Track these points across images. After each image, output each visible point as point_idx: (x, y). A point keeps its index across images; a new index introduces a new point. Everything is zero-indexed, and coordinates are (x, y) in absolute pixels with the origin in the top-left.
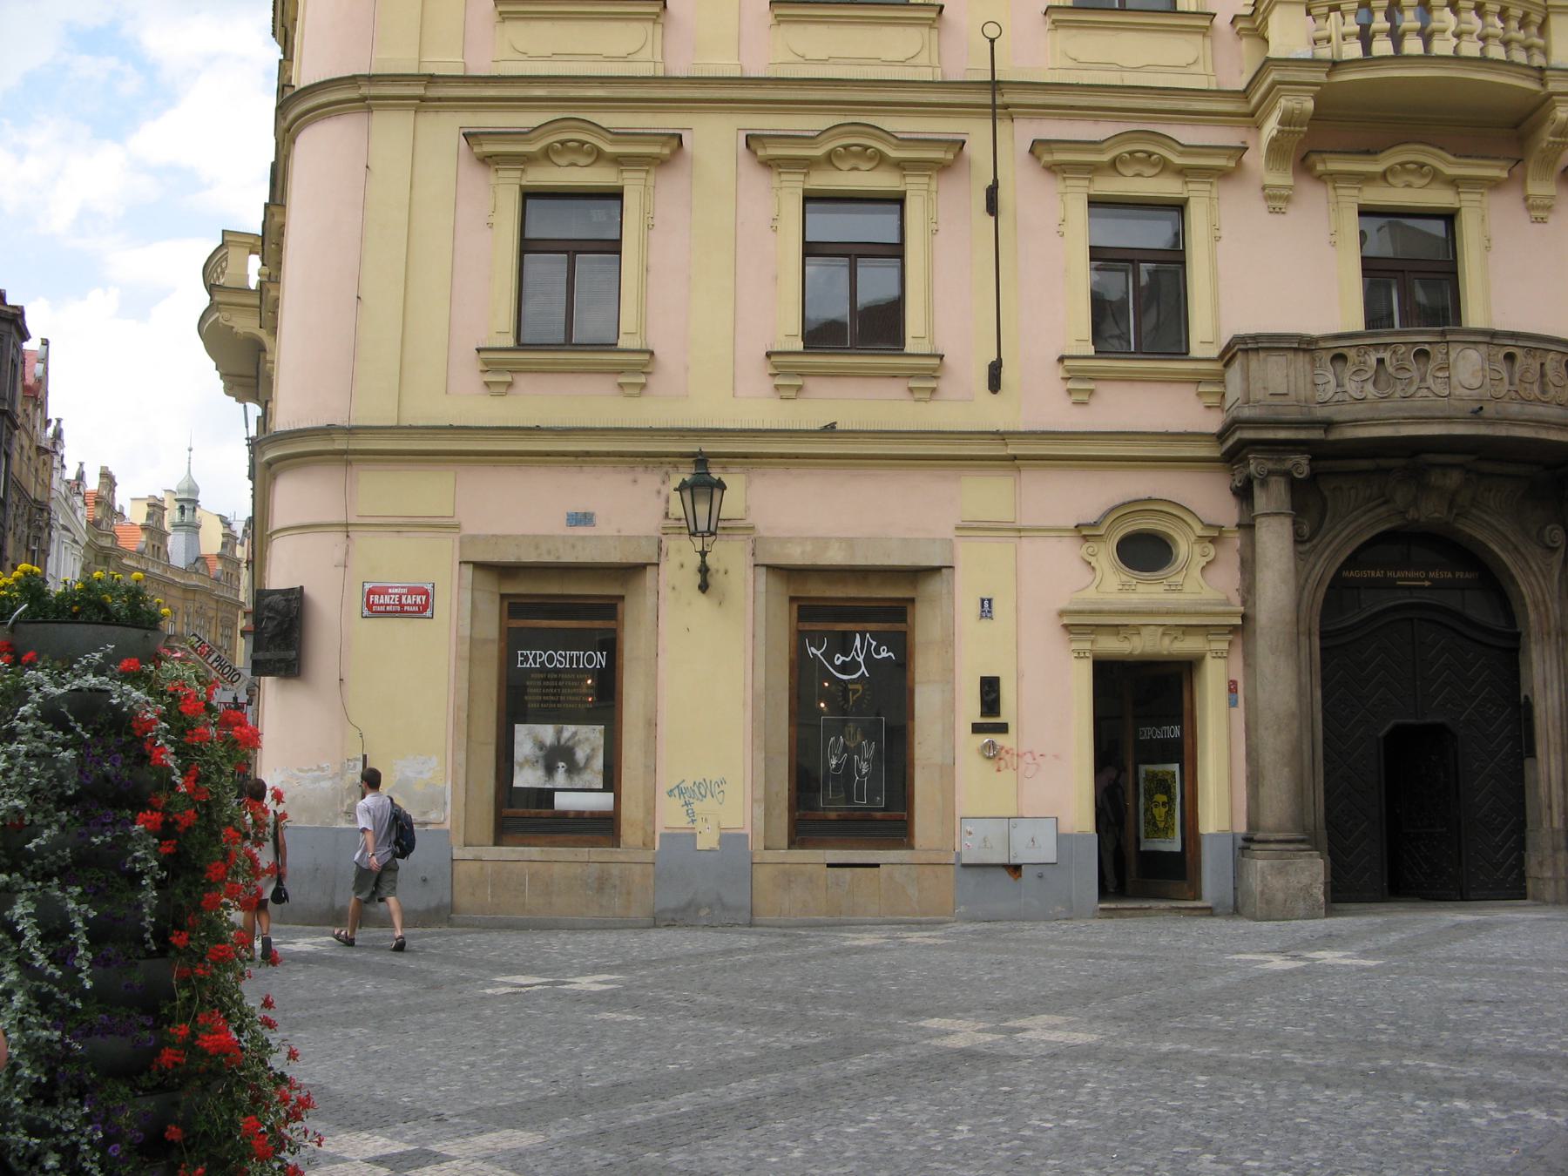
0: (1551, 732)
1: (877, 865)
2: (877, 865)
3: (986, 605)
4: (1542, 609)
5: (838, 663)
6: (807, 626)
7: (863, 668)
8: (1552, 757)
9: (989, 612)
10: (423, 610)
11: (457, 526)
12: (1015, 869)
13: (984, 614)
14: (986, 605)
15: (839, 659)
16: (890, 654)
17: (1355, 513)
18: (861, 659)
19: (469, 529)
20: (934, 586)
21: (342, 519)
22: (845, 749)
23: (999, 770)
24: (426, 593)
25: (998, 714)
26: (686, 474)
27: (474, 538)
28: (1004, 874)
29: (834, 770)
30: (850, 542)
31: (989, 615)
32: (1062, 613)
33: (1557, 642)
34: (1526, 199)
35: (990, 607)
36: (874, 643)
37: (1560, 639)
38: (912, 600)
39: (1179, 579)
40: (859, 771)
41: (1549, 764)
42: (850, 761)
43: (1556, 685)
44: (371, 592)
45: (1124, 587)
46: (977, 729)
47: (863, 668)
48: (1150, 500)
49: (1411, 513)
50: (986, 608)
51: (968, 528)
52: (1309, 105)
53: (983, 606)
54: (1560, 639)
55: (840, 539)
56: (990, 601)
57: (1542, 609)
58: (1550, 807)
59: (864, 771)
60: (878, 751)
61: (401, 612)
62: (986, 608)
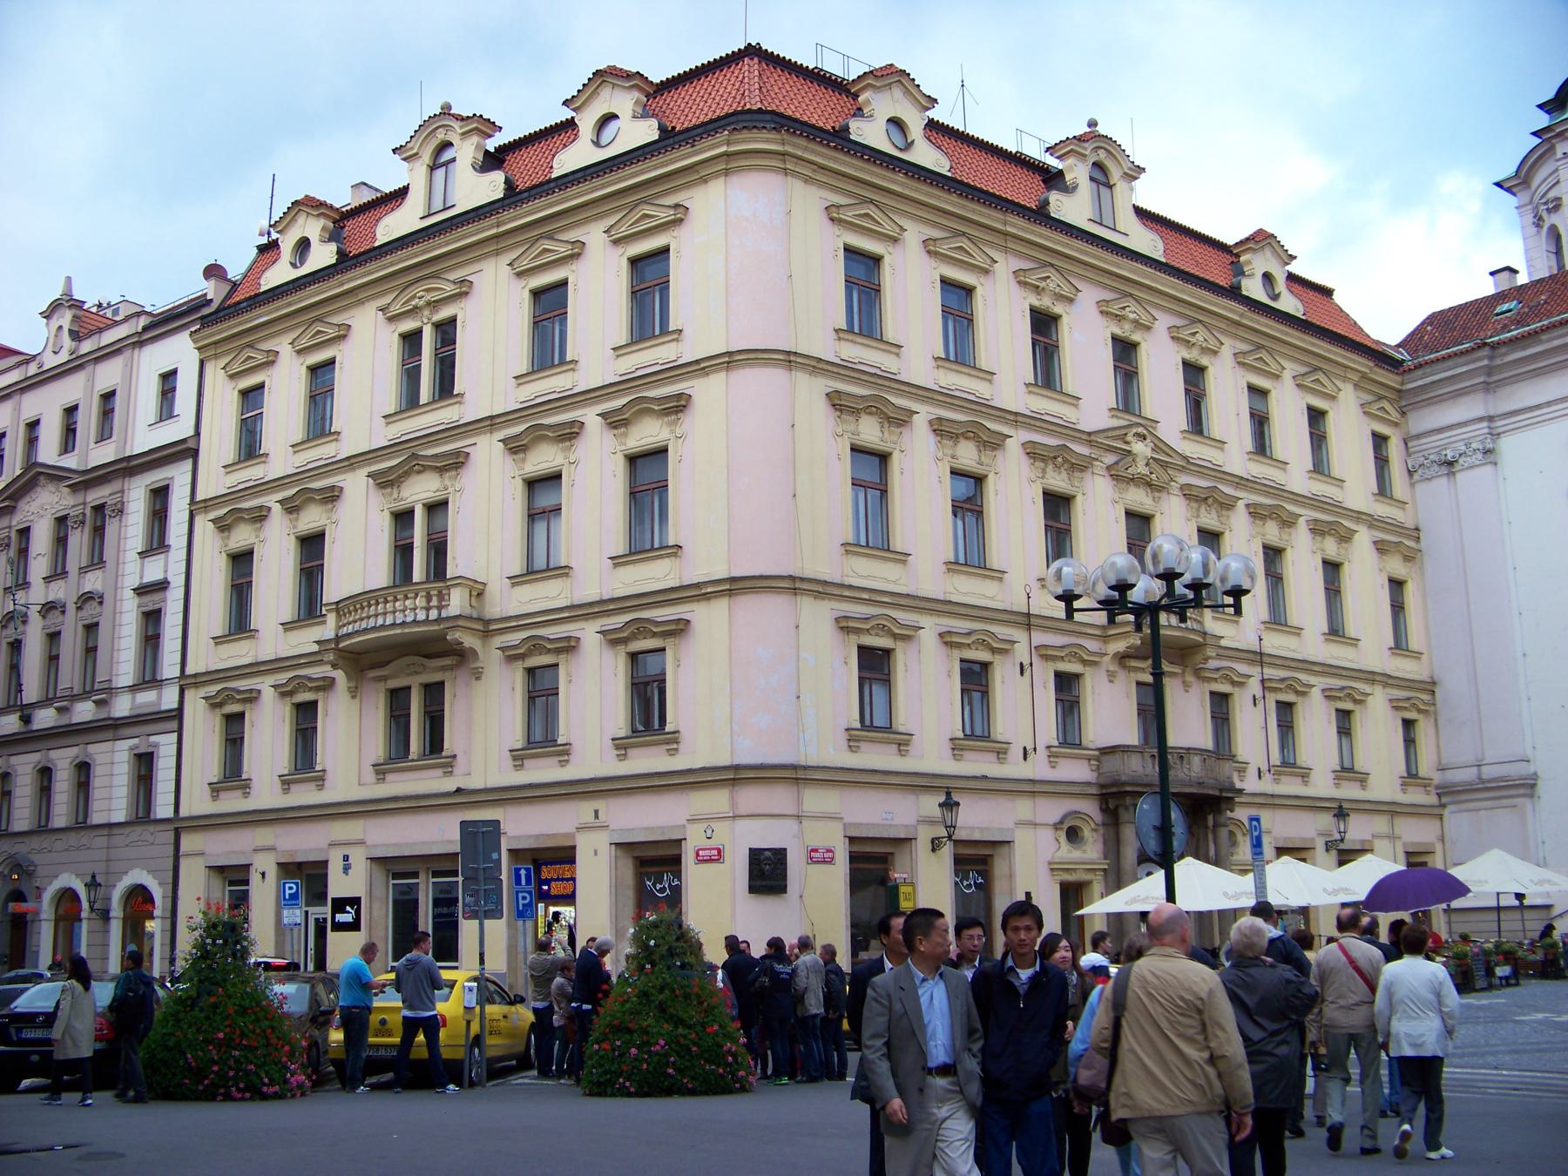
10: (831, 861)
11: (842, 818)
15: (965, 883)
19: (847, 820)
20: (1004, 850)
21: (795, 813)
24: (831, 851)
26: (942, 799)
27: (850, 824)
30: (982, 829)
32: (1050, 863)
34: (1184, 682)
39: (1084, 848)
44: (813, 850)
45: (1069, 851)
48: (1076, 812)
51: (1021, 824)
52: (1139, 642)
61: (824, 862)
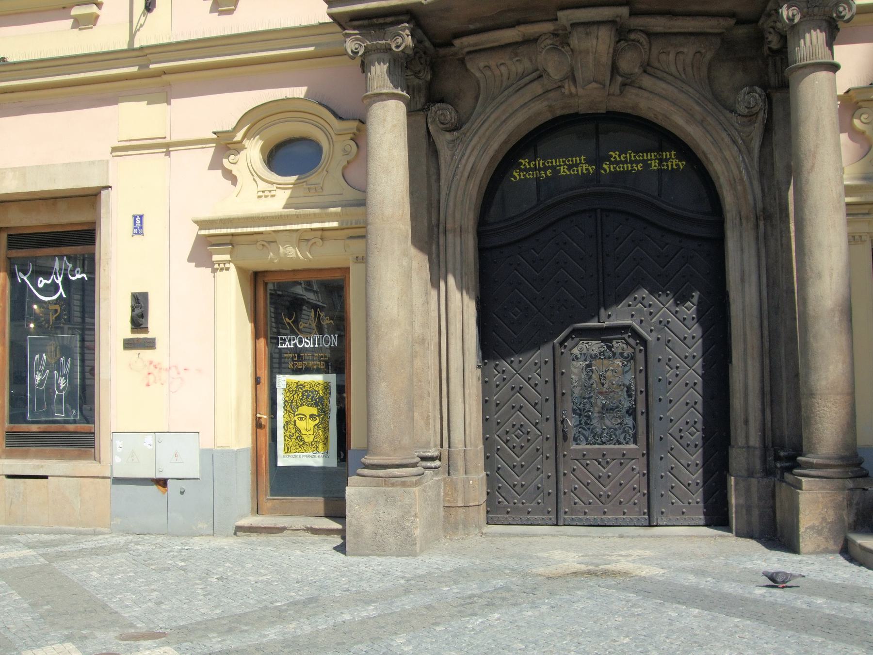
0: (748, 332)
1: (46, 477)
2: (46, 477)
3: (138, 222)
4: (739, 188)
5: (41, 286)
6: (15, 253)
7: (61, 290)
8: (750, 362)
9: (141, 228)
12: (162, 483)
13: (136, 231)
14: (138, 222)
15: (42, 282)
16: (84, 275)
17: (506, 93)
18: (59, 281)
22: (48, 365)
23: (148, 385)
25: (145, 330)
28: (154, 488)
29: (40, 385)
30: (22, 172)
31: (140, 231)
32: (203, 224)
33: (757, 226)
35: (141, 223)
36: (70, 266)
37: (761, 223)
38: (94, 223)
40: (58, 386)
41: (746, 370)
42: (51, 377)
43: (754, 278)
46: (129, 345)
47: (61, 290)
49: (566, 86)
50: (138, 224)
53: (135, 221)
54: (761, 223)
55: (14, 169)
56: (141, 217)
57: (739, 188)
58: (746, 422)
59: (62, 386)
60: (73, 365)
62: (138, 224)
